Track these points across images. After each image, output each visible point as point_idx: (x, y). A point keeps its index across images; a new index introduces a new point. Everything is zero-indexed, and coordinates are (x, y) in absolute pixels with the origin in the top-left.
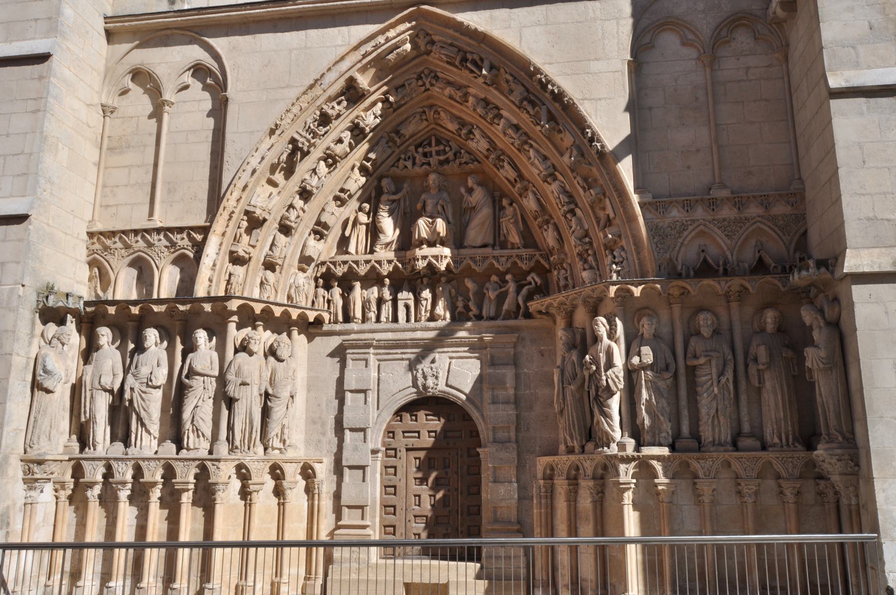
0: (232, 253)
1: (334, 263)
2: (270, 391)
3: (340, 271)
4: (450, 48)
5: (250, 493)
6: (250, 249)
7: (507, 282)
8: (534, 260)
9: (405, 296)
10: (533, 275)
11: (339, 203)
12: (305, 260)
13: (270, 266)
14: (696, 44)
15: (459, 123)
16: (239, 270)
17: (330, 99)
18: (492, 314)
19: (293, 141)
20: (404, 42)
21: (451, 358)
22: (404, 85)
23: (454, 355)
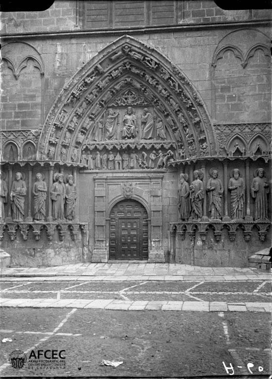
0: (50, 141)
1: (89, 144)
2: (67, 197)
3: (92, 148)
4: (138, 54)
5: (62, 236)
6: (57, 140)
7: (159, 153)
8: (170, 145)
9: (118, 157)
10: (170, 151)
11: (91, 119)
12: (78, 143)
13: (65, 146)
14: (240, 57)
15: (141, 86)
16: (52, 149)
17: (88, 76)
18: (153, 167)
19: (73, 94)
20: (119, 51)
21: (136, 184)
22: (118, 69)
23: (138, 183)
